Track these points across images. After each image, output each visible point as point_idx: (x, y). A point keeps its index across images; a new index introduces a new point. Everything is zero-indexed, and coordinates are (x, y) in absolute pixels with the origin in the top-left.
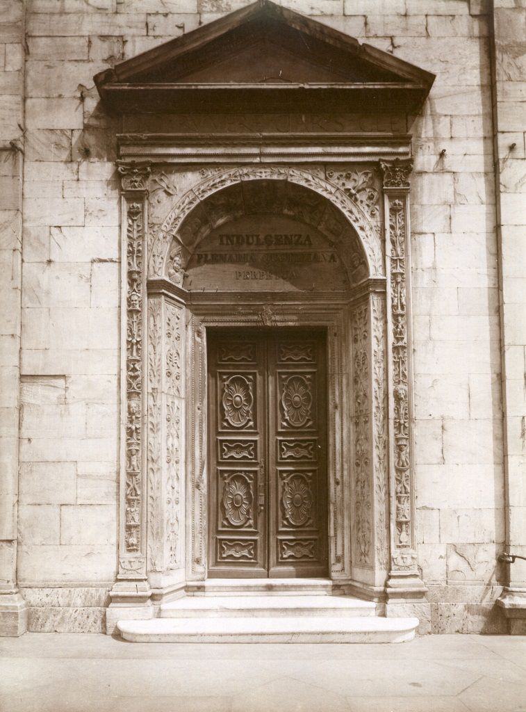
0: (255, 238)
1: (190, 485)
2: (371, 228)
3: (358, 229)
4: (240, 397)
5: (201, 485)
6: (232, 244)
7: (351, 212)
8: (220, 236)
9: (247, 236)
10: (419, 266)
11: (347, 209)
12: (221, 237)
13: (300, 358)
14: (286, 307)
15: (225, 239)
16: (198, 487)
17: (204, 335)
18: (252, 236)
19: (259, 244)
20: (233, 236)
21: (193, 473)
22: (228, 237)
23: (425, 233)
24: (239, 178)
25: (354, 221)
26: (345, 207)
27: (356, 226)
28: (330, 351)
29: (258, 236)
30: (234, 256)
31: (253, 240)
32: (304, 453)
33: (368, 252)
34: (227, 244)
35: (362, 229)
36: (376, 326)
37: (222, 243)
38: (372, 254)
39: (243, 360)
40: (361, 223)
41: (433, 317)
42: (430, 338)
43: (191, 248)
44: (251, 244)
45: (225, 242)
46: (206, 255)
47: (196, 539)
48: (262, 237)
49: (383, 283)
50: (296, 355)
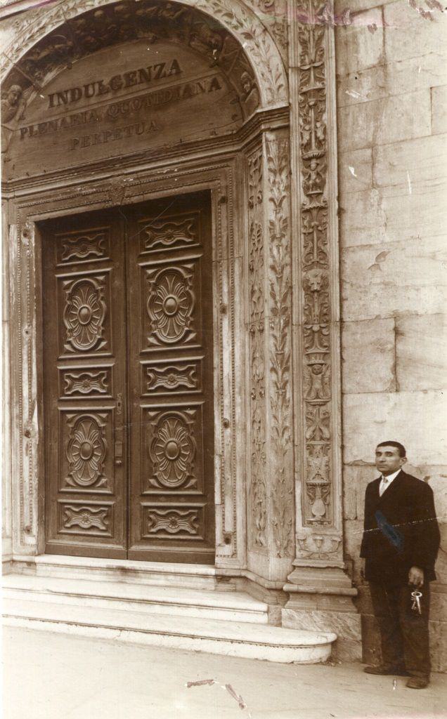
0: (97, 87)
1: (17, 432)
2: (265, 30)
3: (240, 38)
4: (88, 309)
5: (32, 433)
6: (65, 102)
7: (230, 15)
8: (49, 95)
9: (84, 86)
10: (353, 68)
11: (224, 12)
12: (51, 97)
13: (174, 241)
14: (143, 174)
15: (55, 98)
16: (28, 434)
17: (33, 234)
18: (93, 84)
19: (101, 93)
20: (66, 92)
21: (20, 416)
22: (60, 95)
23: (366, 10)
24: (63, 18)
25: (236, 27)
26: (219, 11)
27: (237, 34)
28: (214, 227)
29: (100, 83)
30: (68, 120)
31: (94, 90)
32: (183, 381)
33: (258, 70)
34: (59, 105)
35: (249, 36)
36: (274, 182)
37: (52, 105)
38: (265, 70)
39: (92, 256)
40: (247, 26)
41: (381, 149)
42: (374, 185)
43: (13, 121)
44: (92, 96)
45: (56, 103)
46: (31, 127)
47: (25, 501)
48: (106, 81)
49: (284, 112)
50: (170, 237)
